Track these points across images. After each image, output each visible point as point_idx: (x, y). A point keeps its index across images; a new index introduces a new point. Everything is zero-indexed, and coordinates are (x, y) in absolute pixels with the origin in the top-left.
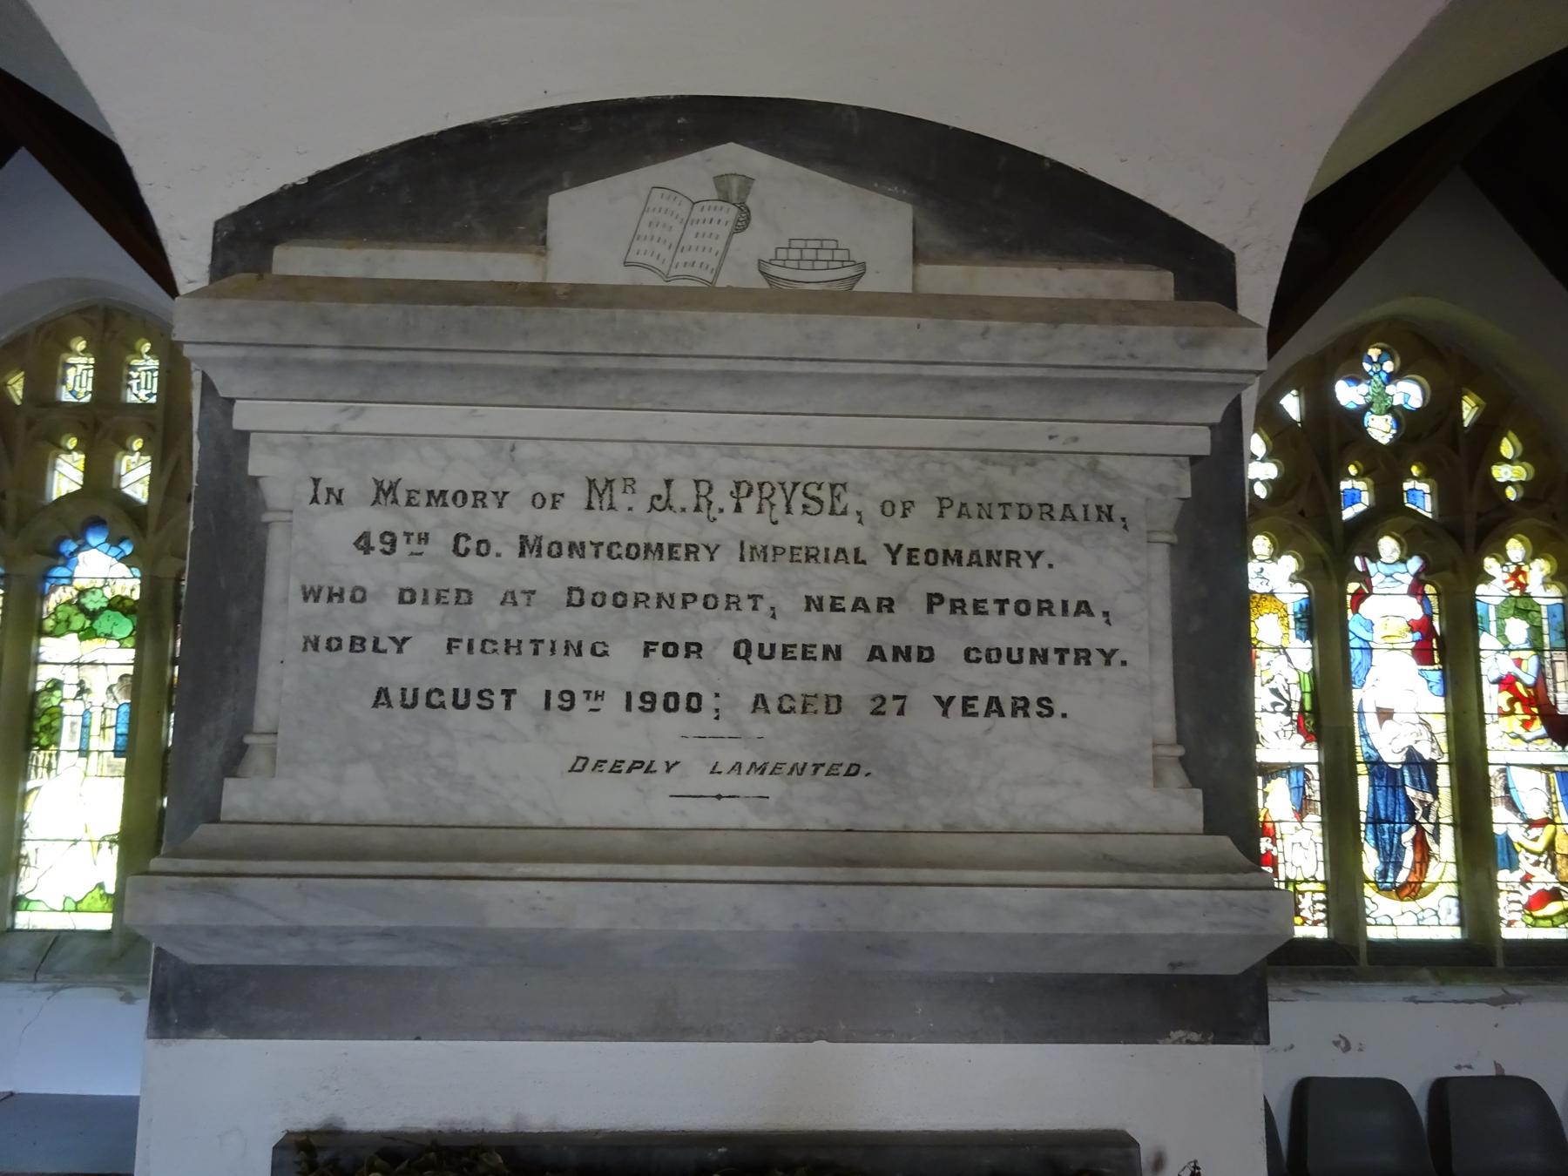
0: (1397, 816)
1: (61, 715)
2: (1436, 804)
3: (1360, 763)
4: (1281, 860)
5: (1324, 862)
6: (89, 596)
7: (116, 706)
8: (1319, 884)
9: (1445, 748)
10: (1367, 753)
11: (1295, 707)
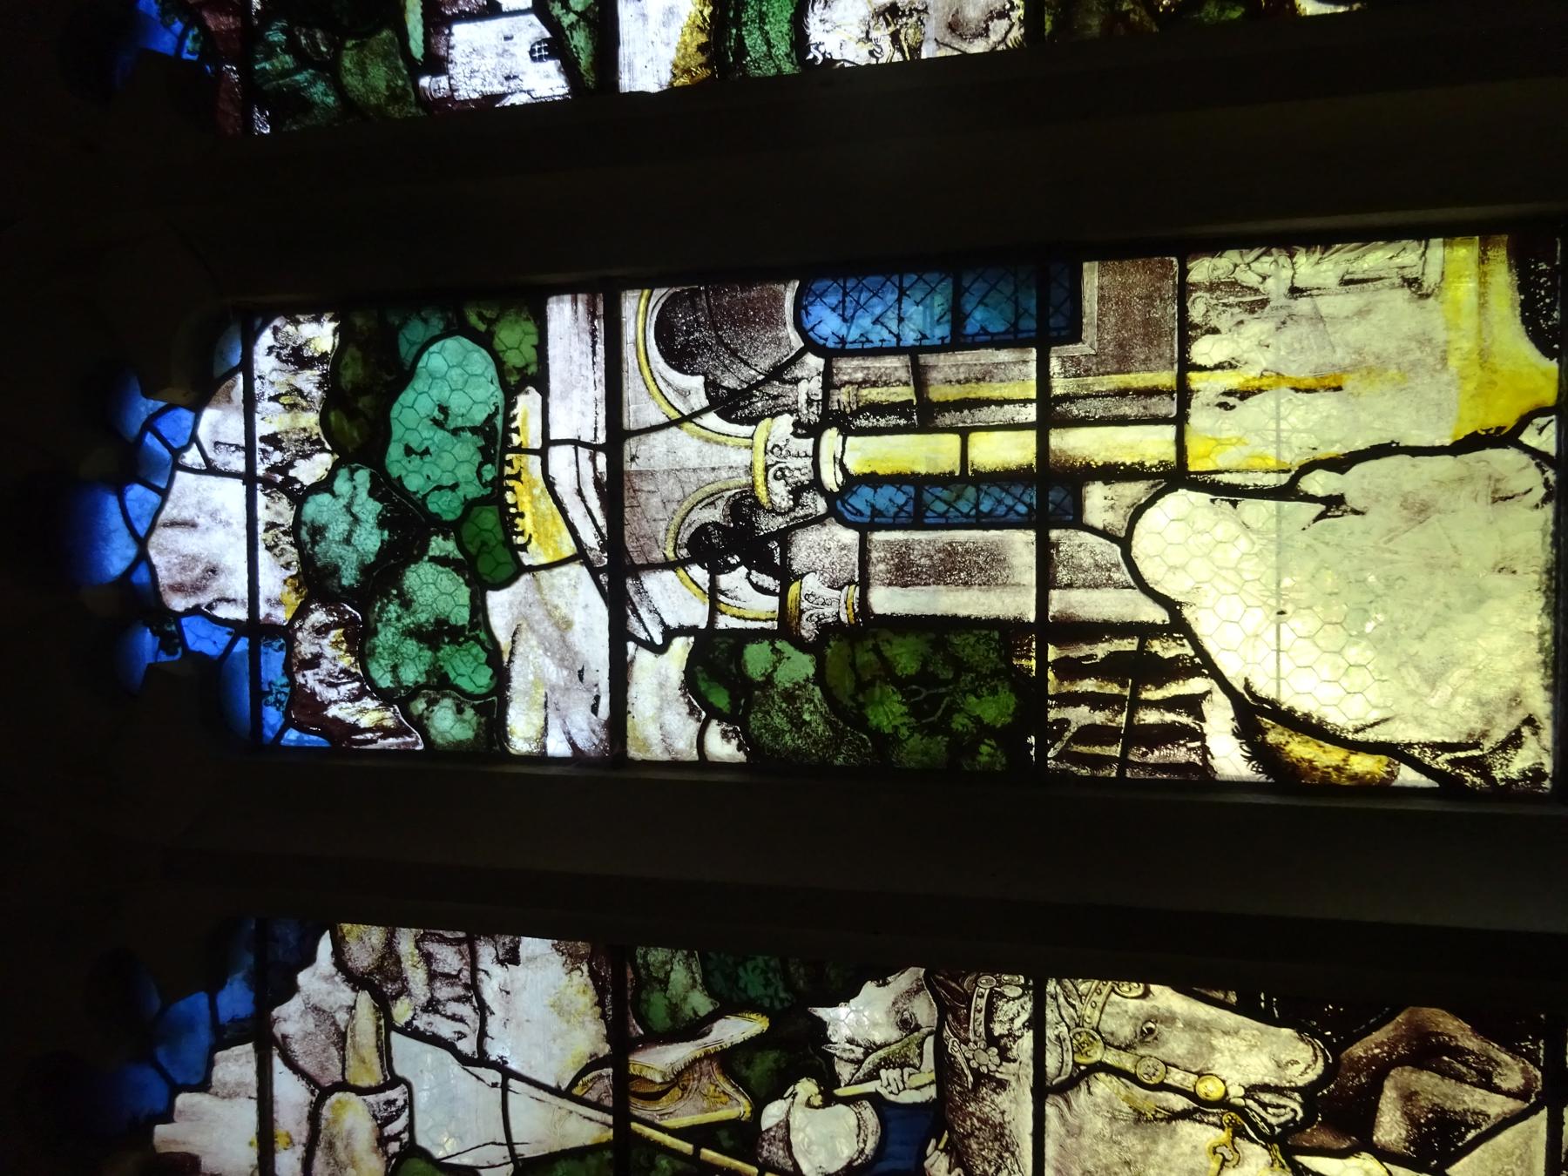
1: (868, 625)
6: (330, 549)
7: (814, 362)
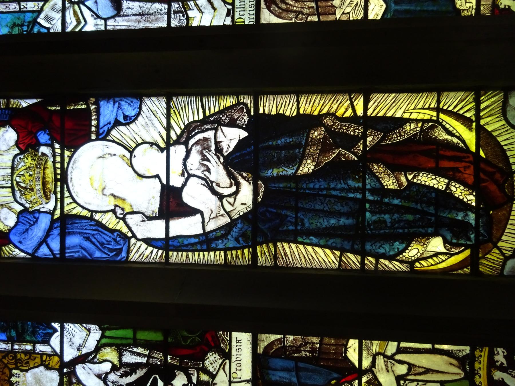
0: (352, 195)
2: (328, 121)
8: (477, 353)
9: (229, 101)
10: (237, 240)
11: (158, 357)
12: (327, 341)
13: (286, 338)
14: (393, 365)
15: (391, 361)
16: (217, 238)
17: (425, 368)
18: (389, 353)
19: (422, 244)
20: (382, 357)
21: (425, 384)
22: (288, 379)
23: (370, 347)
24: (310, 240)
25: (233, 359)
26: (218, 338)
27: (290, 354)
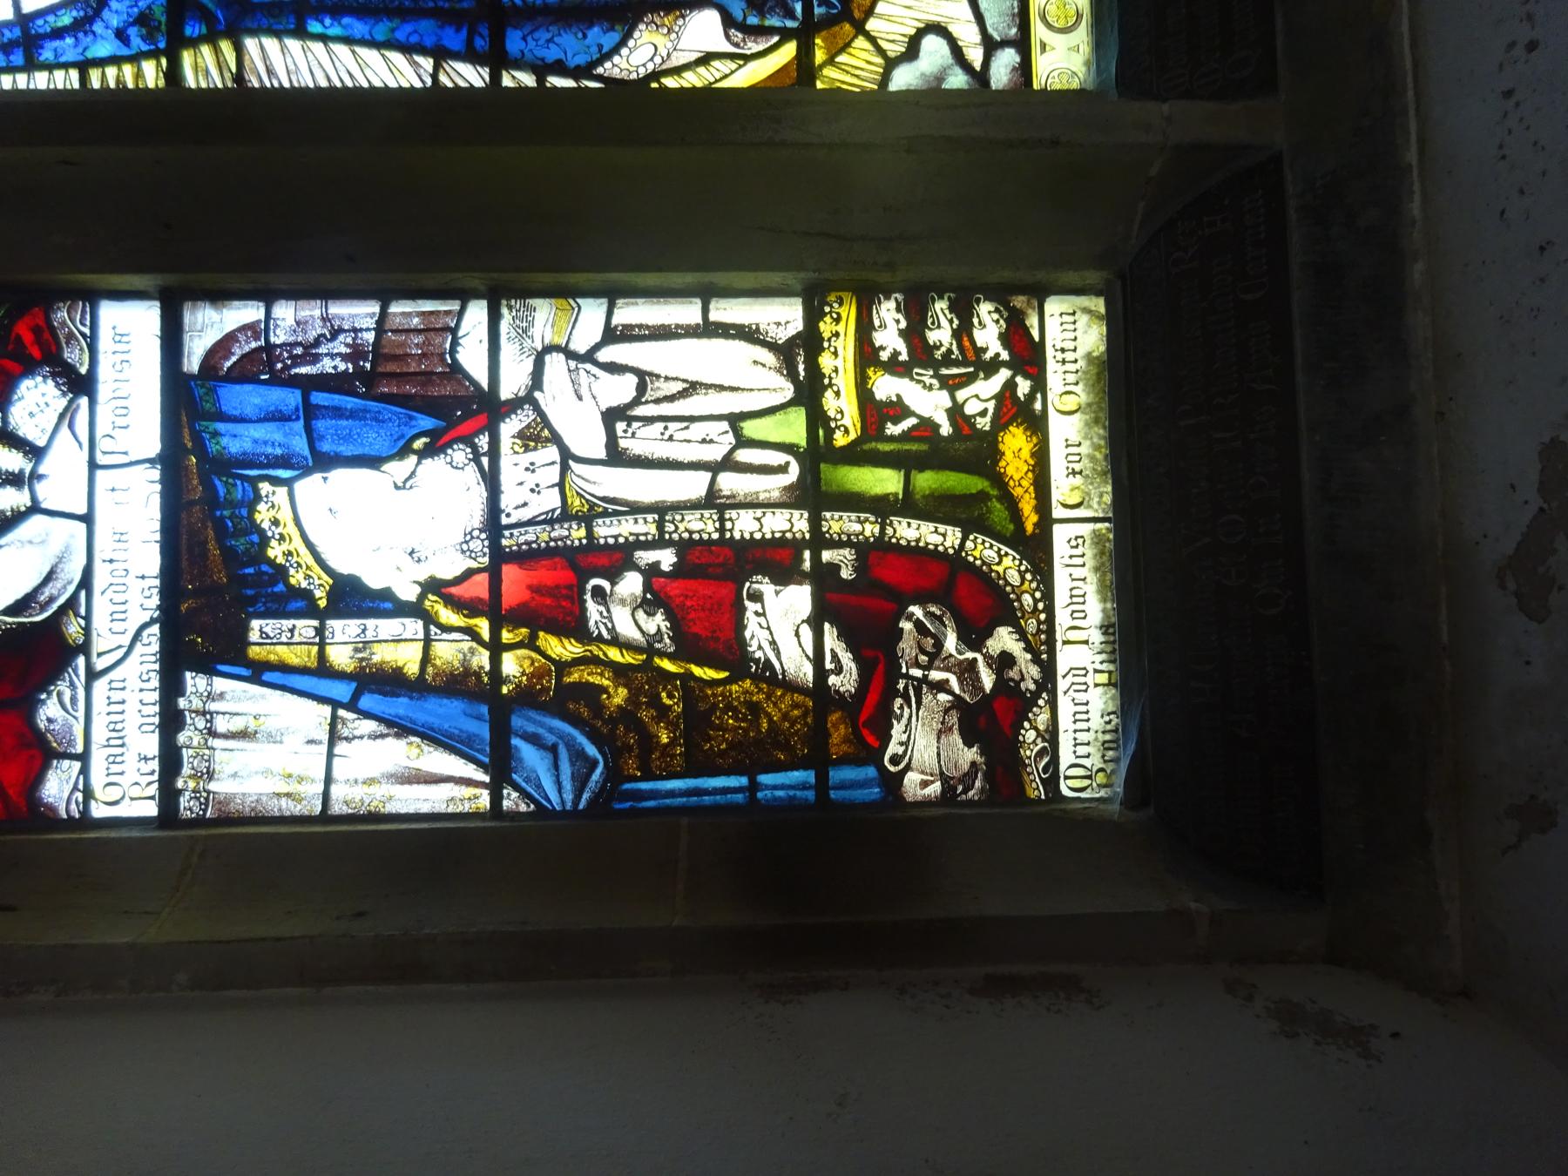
3: (173, 74)
4: (701, 525)
5: (706, 294)
8: (826, 327)
10: (121, 35)
12: (398, 320)
13: (274, 319)
14: (593, 378)
15: (588, 366)
16: (58, 34)
17: (684, 381)
18: (580, 345)
19: (665, 31)
20: (562, 357)
21: (687, 428)
22: (280, 445)
23: (525, 331)
24: (344, 27)
25: (104, 390)
26: (52, 330)
27: (286, 368)
